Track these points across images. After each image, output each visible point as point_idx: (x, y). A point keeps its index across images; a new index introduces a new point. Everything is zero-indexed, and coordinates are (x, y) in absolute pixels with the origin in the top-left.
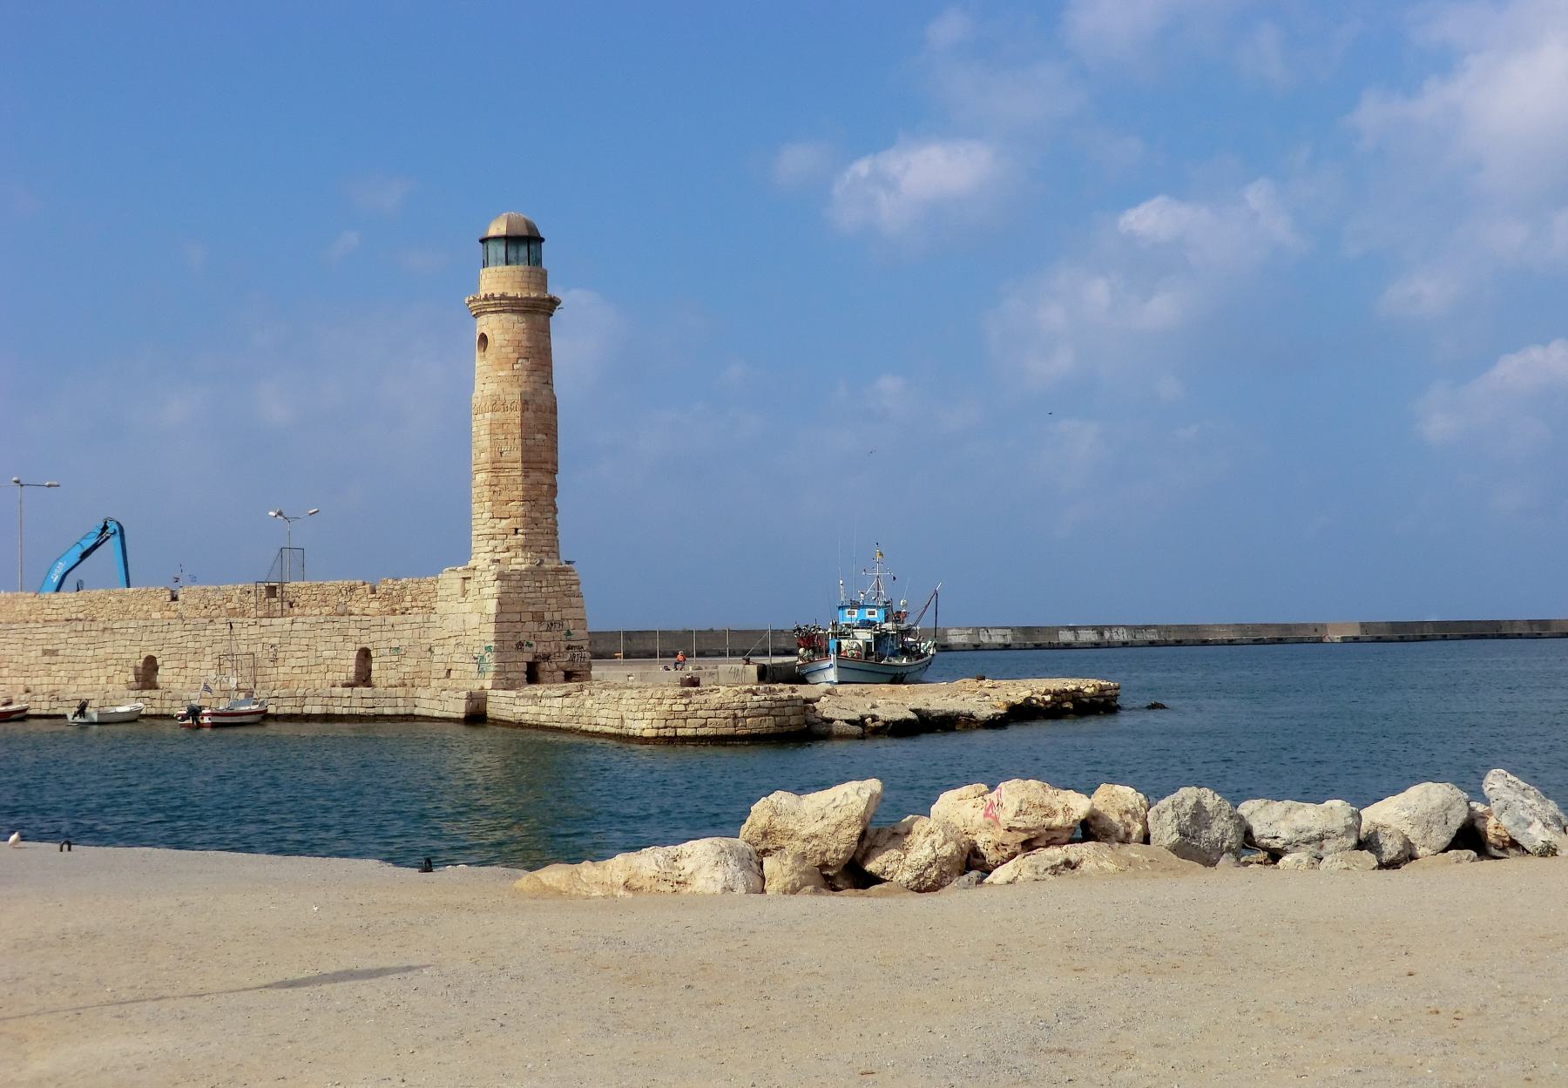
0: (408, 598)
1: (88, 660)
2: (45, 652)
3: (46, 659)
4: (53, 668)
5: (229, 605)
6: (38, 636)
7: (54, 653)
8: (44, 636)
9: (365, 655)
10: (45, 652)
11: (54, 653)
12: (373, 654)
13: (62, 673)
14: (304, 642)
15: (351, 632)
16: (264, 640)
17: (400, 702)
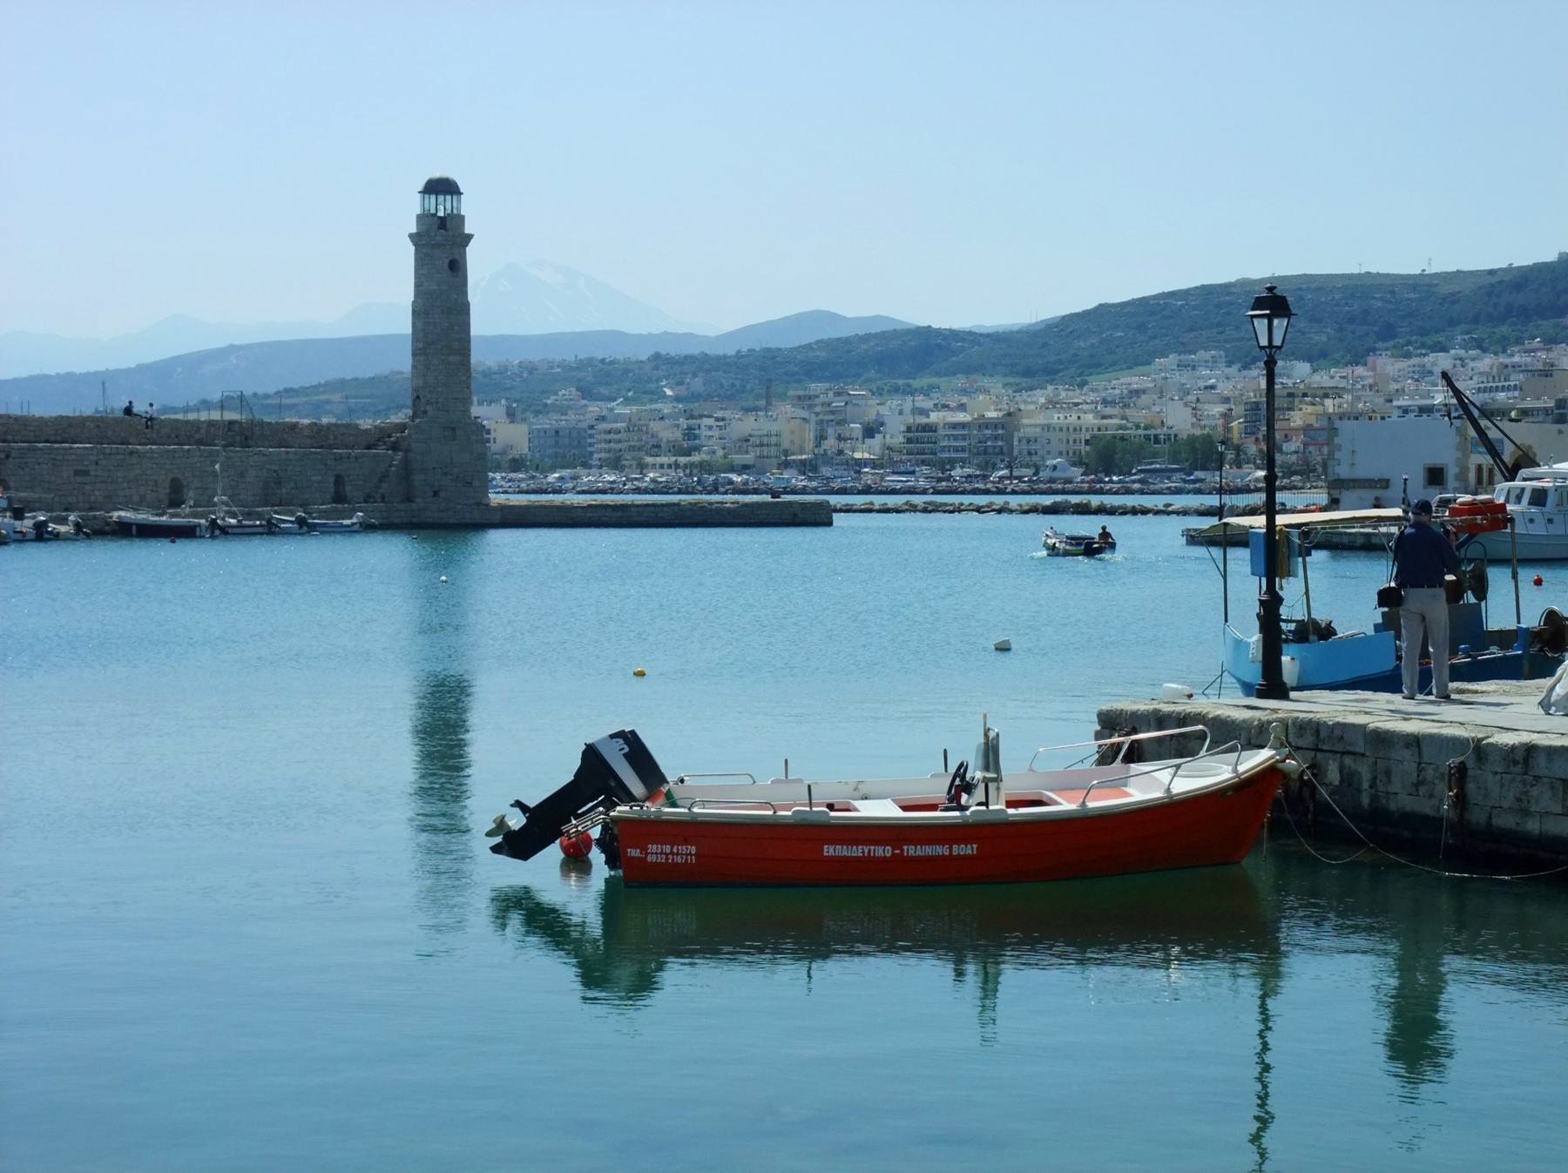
0: (332, 437)
1: (120, 480)
2: (77, 473)
3: (79, 479)
4: (87, 487)
5: (197, 436)
6: (66, 457)
7: (86, 473)
8: (74, 457)
9: (339, 480)
10: (77, 473)
11: (86, 473)
12: (346, 479)
13: (97, 493)
14: (298, 469)
15: (329, 462)
16: (268, 466)
17: (403, 513)
